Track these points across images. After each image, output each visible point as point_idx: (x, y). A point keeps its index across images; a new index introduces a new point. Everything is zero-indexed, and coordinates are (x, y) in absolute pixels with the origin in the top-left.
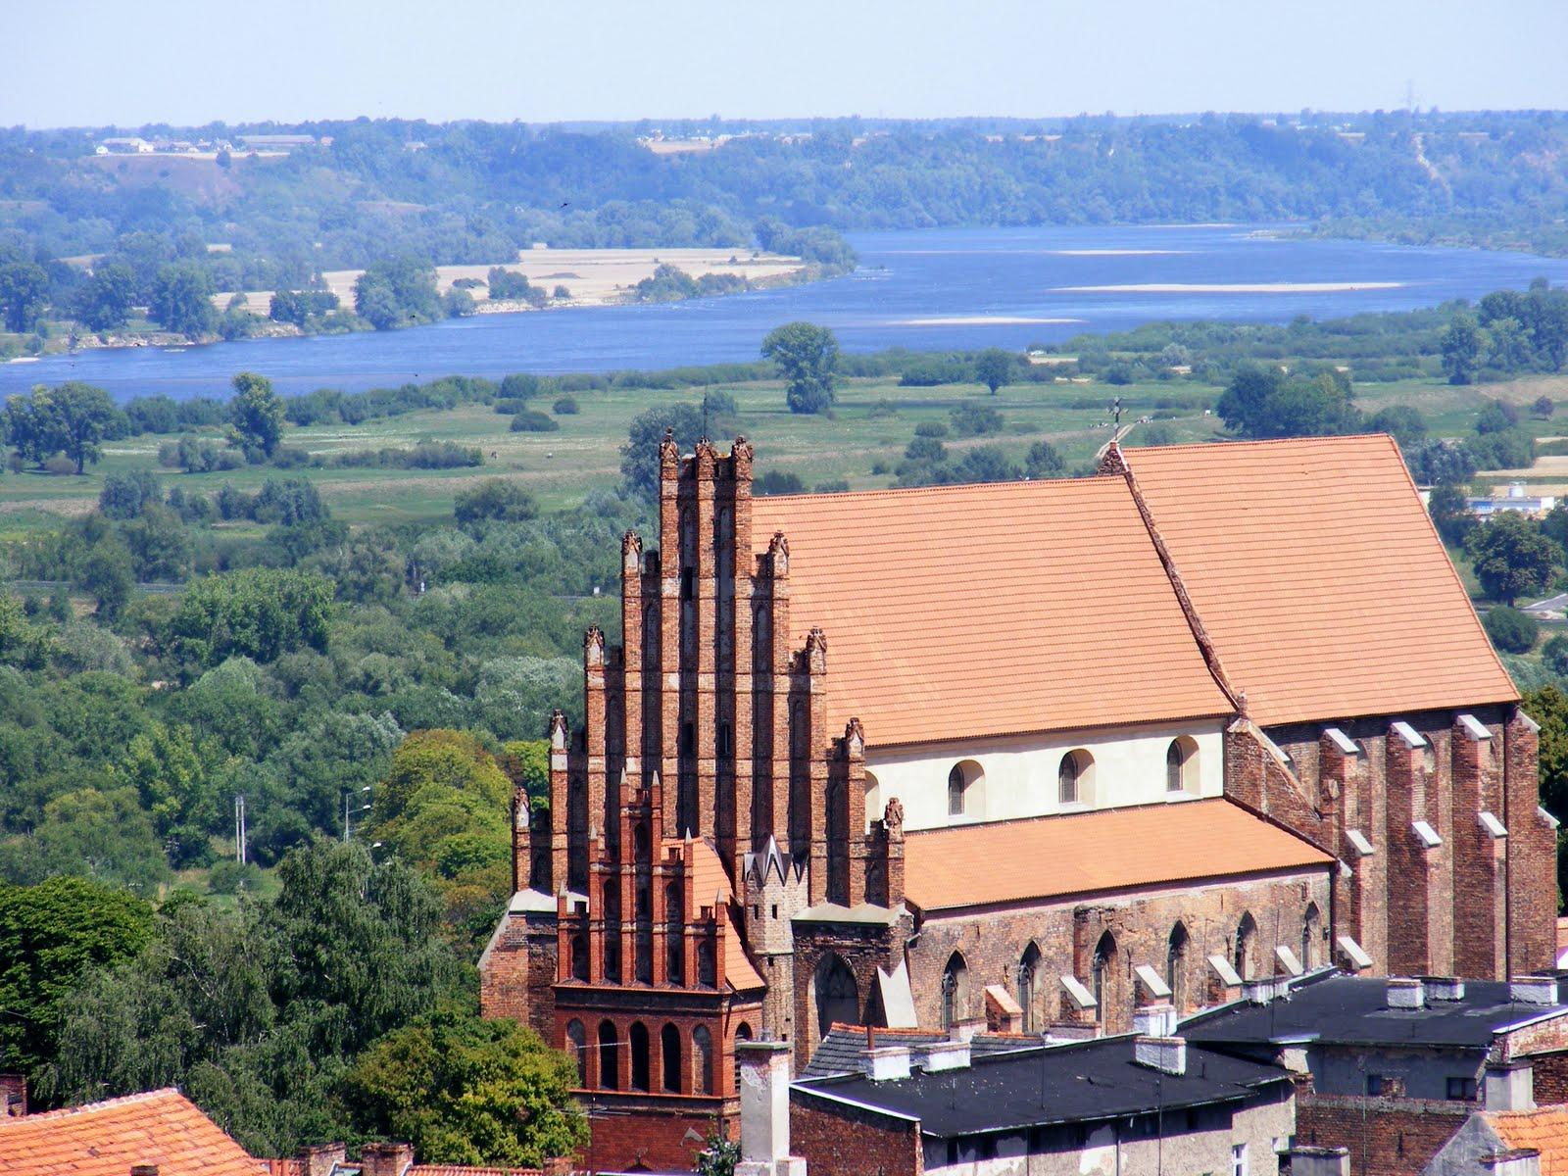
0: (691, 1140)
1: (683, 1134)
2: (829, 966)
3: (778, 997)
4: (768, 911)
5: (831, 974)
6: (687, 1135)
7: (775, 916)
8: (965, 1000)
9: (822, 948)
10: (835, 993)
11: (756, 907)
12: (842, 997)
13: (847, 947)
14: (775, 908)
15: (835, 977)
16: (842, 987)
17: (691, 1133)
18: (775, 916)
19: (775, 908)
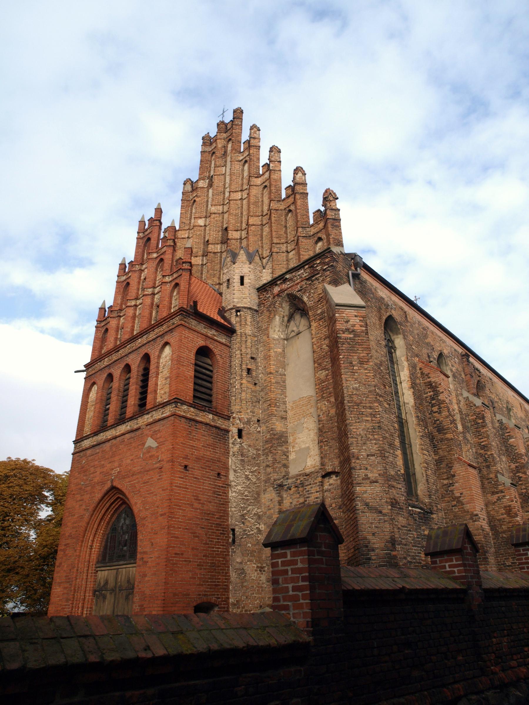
0: (150, 447)
1: (144, 444)
2: (287, 313)
3: (244, 339)
4: (237, 279)
5: (289, 321)
6: (147, 445)
7: (242, 283)
8: (403, 359)
9: (278, 295)
10: (293, 334)
11: (228, 280)
12: (299, 333)
13: (298, 284)
14: (242, 278)
15: (292, 323)
16: (298, 327)
17: (151, 443)
18: (242, 283)
19: (242, 278)
